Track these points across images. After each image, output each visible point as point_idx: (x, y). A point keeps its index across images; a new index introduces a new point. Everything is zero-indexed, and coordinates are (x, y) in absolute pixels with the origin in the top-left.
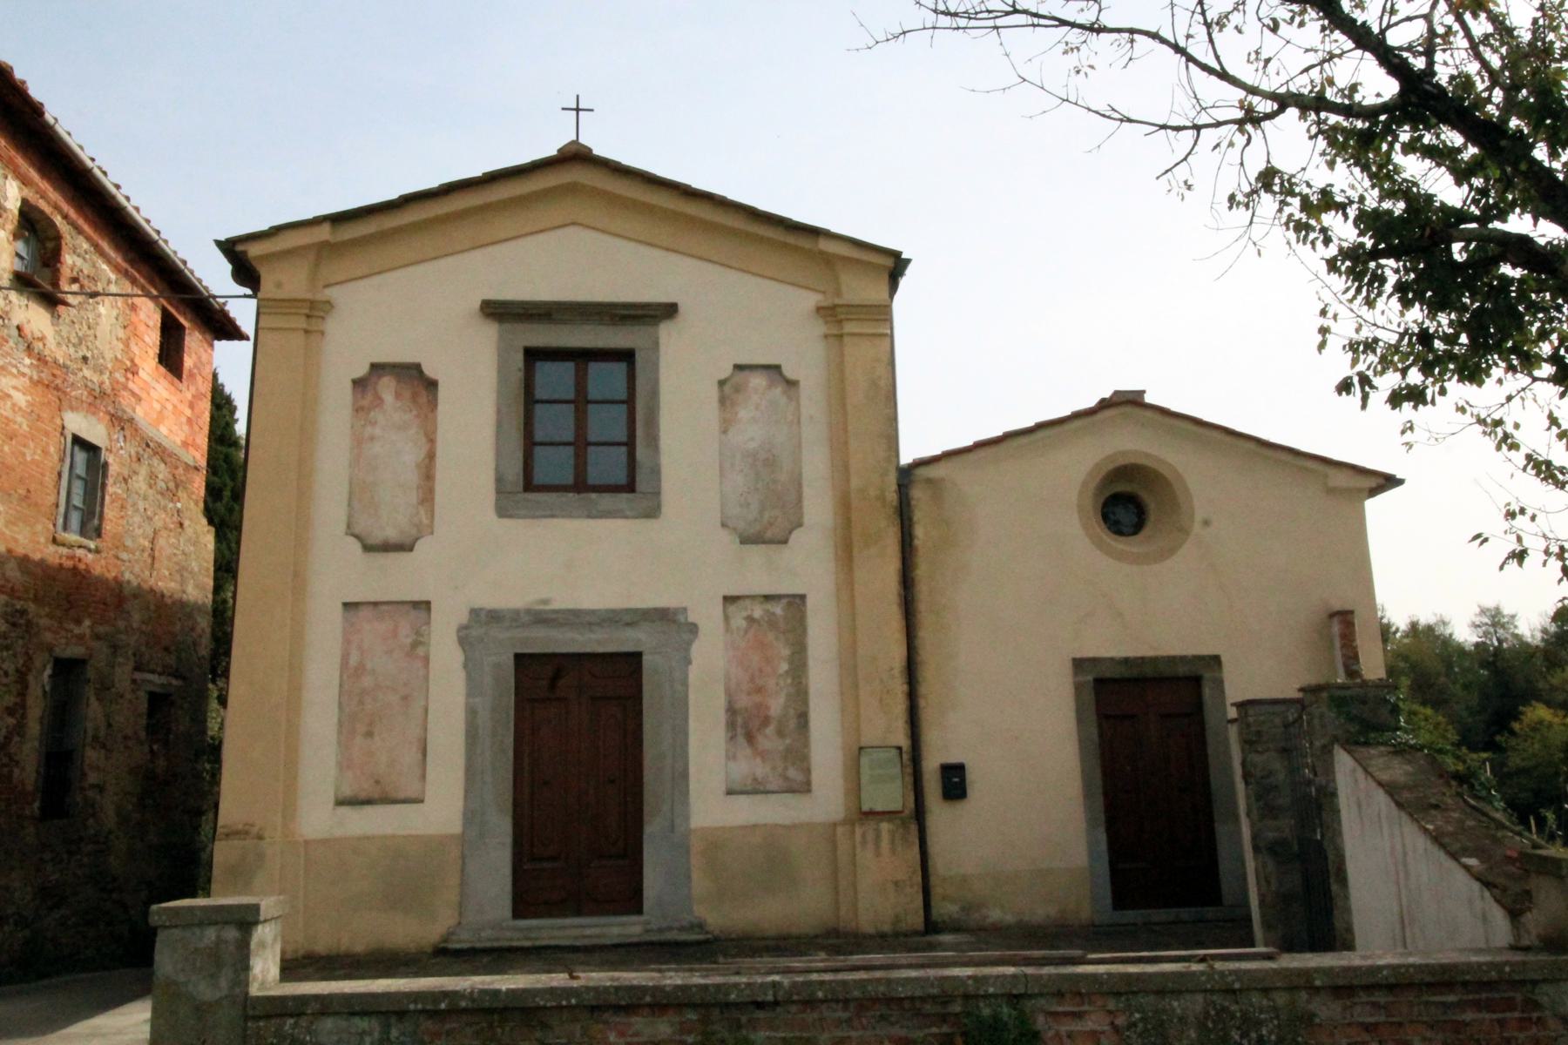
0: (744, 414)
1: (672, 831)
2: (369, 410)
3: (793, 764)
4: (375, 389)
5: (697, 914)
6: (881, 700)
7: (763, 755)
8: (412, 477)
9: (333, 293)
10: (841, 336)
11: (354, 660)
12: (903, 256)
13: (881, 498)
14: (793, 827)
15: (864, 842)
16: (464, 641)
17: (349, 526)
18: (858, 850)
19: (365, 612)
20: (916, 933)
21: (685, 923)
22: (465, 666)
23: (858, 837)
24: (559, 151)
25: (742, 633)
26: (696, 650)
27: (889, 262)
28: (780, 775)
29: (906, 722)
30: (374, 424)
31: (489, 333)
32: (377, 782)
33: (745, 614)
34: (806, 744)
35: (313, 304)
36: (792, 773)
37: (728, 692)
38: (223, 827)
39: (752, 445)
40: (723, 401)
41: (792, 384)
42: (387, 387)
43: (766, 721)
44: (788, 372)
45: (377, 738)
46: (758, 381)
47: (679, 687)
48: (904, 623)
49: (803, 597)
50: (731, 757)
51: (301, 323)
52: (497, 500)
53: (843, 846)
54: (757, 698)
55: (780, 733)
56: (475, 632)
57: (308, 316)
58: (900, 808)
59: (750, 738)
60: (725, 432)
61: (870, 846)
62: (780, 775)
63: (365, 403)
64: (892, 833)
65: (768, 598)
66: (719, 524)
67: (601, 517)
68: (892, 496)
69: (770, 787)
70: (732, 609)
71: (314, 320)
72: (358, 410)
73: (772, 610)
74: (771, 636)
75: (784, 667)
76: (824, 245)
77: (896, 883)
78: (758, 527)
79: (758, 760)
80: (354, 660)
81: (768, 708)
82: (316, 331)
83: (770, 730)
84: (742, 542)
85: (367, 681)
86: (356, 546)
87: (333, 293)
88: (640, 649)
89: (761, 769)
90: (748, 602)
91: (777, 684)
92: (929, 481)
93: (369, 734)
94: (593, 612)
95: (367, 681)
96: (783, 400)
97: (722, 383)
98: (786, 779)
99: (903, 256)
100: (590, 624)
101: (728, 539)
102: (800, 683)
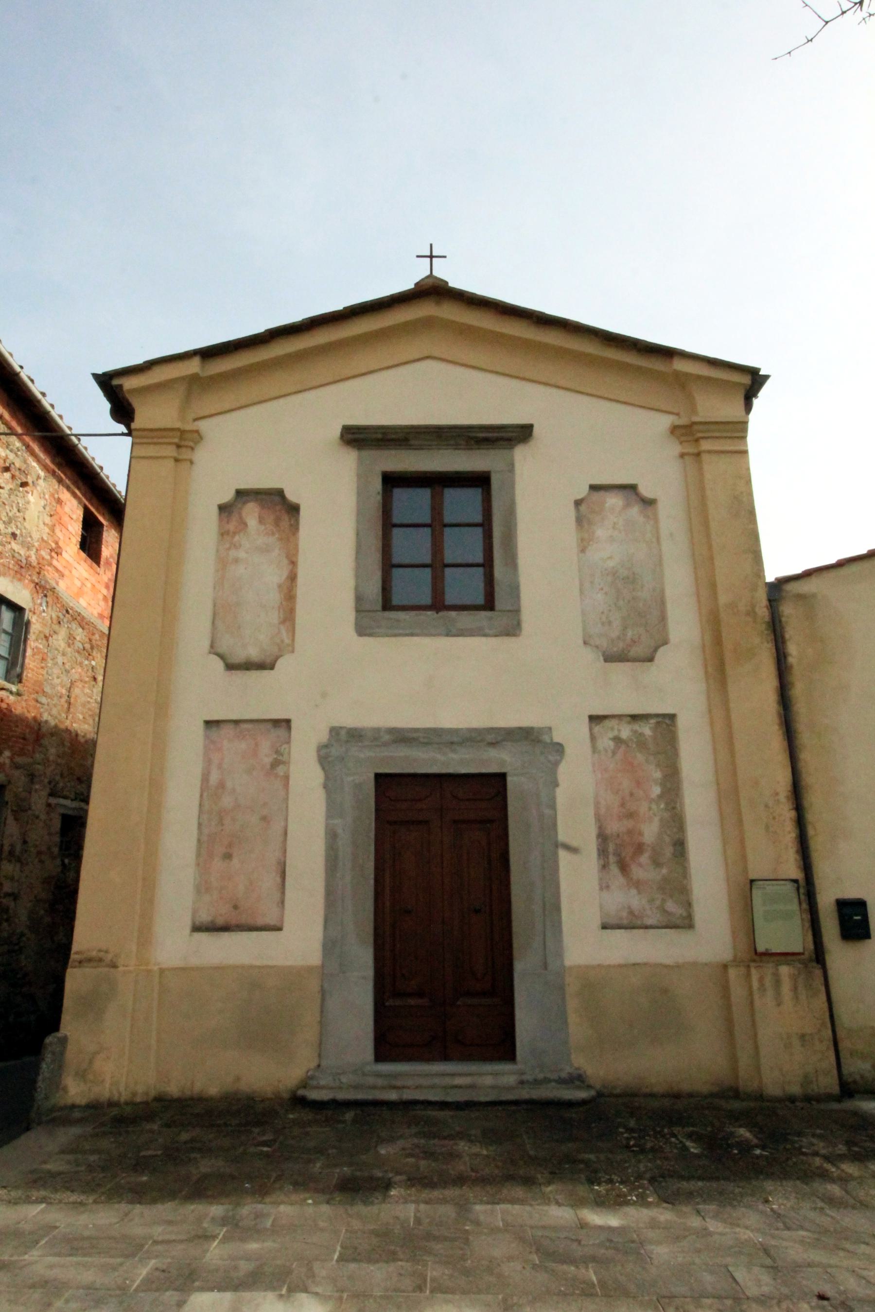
0: (601, 533)
1: (546, 968)
2: (235, 533)
3: (671, 896)
4: (240, 514)
5: (576, 1065)
6: (767, 827)
7: (638, 885)
8: (274, 597)
9: (204, 426)
10: (698, 454)
11: (214, 778)
12: (761, 373)
13: (751, 612)
14: (678, 966)
15: (762, 988)
16: (325, 758)
17: (212, 646)
18: (756, 997)
19: (227, 731)
20: (830, 1097)
21: (564, 1075)
22: (325, 786)
23: (755, 984)
24: (417, 284)
25: (610, 754)
26: (563, 771)
27: (746, 380)
28: (657, 908)
29: (797, 852)
30: (237, 546)
31: (350, 458)
32: (236, 907)
33: (611, 735)
34: (685, 873)
35: (182, 432)
36: (671, 906)
37: (598, 818)
38: (77, 953)
39: (611, 564)
40: (580, 521)
41: (649, 503)
42: (251, 512)
43: (640, 848)
44: (646, 491)
45: (235, 861)
46: (614, 501)
47: (547, 811)
48: (786, 743)
49: (672, 717)
50: (604, 887)
51: (171, 451)
52: (356, 618)
53: (737, 992)
54: (629, 824)
55: (657, 863)
56: (335, 751)
57: (179, 446)
58: (801, 951)
59: (624, 868)
60: (583, 550)
61: (770, 993)
62: (657, 908)
63: (231, 527)
64: (794, 979)
65: (635, 718)
66: (581, 642)
67: (458, 636)
68: (763, 611)
69: (649, 922)
70: (597, 729)
71: (184, 450)
72: (223, 534)
73: (640, 731)
74: (640, 757)
75: (656, 790)
76: (679, 365)
77: (802, 1037)
78: (621, 645)
79: (634, 891)
80: (214, 778)
81: (641, 834)
82: (186, 460)
83: (644, 859)
84: (606, 660)
85: (227, 801)
86: (220, 665)
87: (204, 426)
88: (503, 771)
89: (636, 901)
90: (613, 723)
91: (650, 809)
92: (801, 597)
93: (228, 856)
94: (455, 731)
95: (227, 801)
96: (641, 519)
97: (578, 503)
98: (665, 912)
99: (761, 373)
100: (452, 743)
101: (590, 658)
102: (674, 808)
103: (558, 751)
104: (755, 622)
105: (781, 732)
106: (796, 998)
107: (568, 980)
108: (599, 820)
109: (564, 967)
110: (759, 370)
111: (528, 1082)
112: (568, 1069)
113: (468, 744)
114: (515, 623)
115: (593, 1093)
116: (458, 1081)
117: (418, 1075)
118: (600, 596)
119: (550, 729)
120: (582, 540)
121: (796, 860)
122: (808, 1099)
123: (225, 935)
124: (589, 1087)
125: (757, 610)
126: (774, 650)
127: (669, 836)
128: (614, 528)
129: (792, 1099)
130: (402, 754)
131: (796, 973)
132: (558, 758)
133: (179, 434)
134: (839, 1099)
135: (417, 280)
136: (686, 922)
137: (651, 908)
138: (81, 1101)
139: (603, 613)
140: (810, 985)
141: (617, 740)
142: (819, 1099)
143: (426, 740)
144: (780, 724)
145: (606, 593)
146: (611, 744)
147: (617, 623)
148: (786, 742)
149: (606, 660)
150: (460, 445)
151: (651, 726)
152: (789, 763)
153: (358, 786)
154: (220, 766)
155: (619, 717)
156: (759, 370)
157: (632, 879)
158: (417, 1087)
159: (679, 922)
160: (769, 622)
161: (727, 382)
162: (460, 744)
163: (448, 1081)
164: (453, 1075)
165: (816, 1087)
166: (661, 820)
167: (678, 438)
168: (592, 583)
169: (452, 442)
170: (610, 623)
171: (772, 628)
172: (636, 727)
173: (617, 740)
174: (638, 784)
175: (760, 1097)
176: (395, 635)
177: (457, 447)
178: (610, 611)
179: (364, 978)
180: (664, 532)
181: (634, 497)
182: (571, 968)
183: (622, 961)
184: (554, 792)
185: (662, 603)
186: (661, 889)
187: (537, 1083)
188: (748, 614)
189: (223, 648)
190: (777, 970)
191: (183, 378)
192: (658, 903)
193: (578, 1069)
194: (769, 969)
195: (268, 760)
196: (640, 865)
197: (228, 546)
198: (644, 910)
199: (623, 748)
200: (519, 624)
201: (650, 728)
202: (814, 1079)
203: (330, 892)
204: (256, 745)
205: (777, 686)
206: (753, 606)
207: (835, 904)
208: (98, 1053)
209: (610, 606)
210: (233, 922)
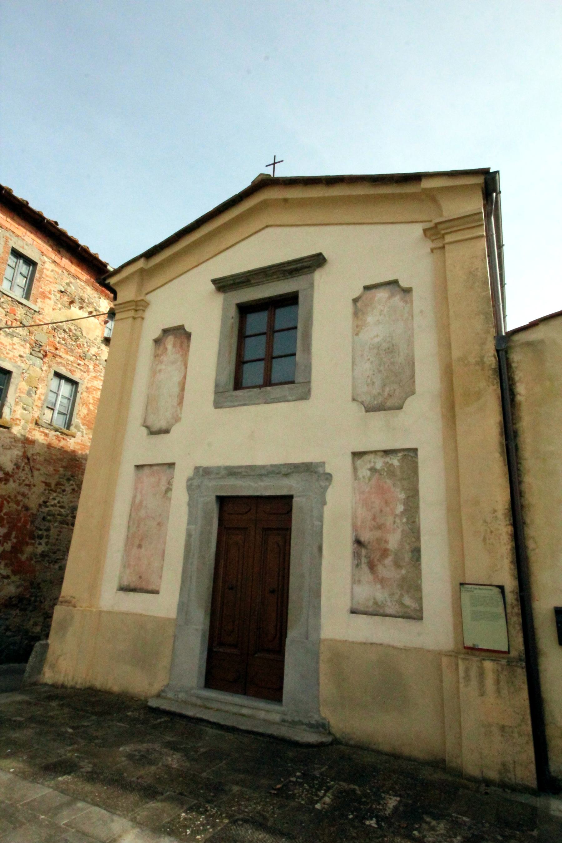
0: (370, 319)
1: (307, 639)
2: (161, 355)
3: (408, 592)
4: (164, 344)
5: (323, 715)
6: (484, 540)
7: (382, 581)
8: (176, 390)
9: (149, 298)
10: (443, 247)
11: (137, 501)
12: (491, 171)
13: (481, 363)
14: (405, 650)
15: (467, 677)
16: (190, 488)
17: (145, 422)
18: (461, 686)
19: (147, 471)
20: (525, 789)
21: (313, 722)
22: (189, 505)
23: (461, 673)
24: (252, 182)
25: (367, 481)
27: (480, 180)
28: (396, 601)
29: (512, 562)
30: (161, 362)
31: (220, 298)
32: (140, 577)
33: (369, 466)
34: (419, 575)
35: (136, 303)
36: (407, 601)
37: (355, 528)
38: (63, 597)
39: (376, 340)
40: (356, 314)
41: (407, 291)
42: (170, 342)
43: (385, 553)
44: (404, 284)
45: (143, 549)
46: (382, 294)
47: (317, 523)
48: (506, 469)
49: (415, 451)
50: (355, 581)
51: (132, 313)
52: (215, 398)
53: (448, 677)
54: (378, 534)
55: (397, 565)
56: (196, 482)
57: (136, 310)
58: (505, 649)
59: (372, 567)
60: (357, 334)
61: (474, 683)
62: (396, 601)
63: (160, 352)
64: (498, 673)
65: (387, 452)
66: (350, 398)
67: (272, 403)
68: (491, 360)
69: (389, 611)
70: (359, 462)
71: (139, 312)
72: (156, 356)
73: (390, 462)
74: (389, 482)
75: (400, 508)
76: (426, 184)
77: (503, 728)
78: (380, 399)
79: (379, 586)
80: (137, 501)
81: (386, 542)
82: (139, 317)
83: (388, 561)
84: (367, 411)
85: (142, 513)
86: (144, 431)
87: (149, 298)
88: (291, 493)
89: (381, 595)
90: (372, 457)
91: (394, 522)
92: (529, 344)
93: (140, 546)
94: (263, 467)
95: (142, 513)
96: (401, 304)
97: (355, 301)
98: (402, 604)
99: (491, 171)
100: (261, 475)
101: (356, 410)
102: (414, 522)
103: (327, 479)
104: (483, 369)
105: (502, 459)
106: (498, 691)
107: (322, 648)
108: (356, 530)
109: (320, 639)
110: (489, 169)
111: (287, 721)
112: (316, 717)
113: (271, 475)
114: (307, 390)
115: (329, 739)
116: (244, 711)
117: (221, 702)
118: (367, 366)
119: (324, 463)
120: (357, 326)
121: (510, 569)
122: (503, 785)
123: (132, 594)
124: (330, 733)
125: (485, 359)
126: (499, 391)
127: (409, 544)
128: (380, 315)
129: (488, 783)
130: (232, 483)
131: (500, 669)
132: (327, 484)
133: (134, 303)
134: (535, 793)
135: (252, 181)
136: (418, 614)
137: (391, 601)
138: (50, 682)
139: (368, 376)
140: (512, 683)
141: (373, 470)
142: (514, 788)
143: (245, 474)
144: (502, 453)
145: (372, 363)
146: (369, 473)
147: (378, 383)
148: (507, 467)
149: (367, 411)
150: (280, 277)
151: (399, 458)
152: (508, 485)
153: (206, 504)
154: (141, 492)
155: (375, 452)
156: (489, 169)
157: (377, 576)
158: (217, 710)
159: (412, 614)
160: (495, 369)
161: (466, 186)
162: (267, 475)
163: (235, 709)
164: (242, 706)
165: (513, 776)
166: (403, 531)
167: (430, 238)
168: (362, 355)
169: (275, 277)
170: (373, 383)
171: (498, 373)
172: (387, 459)
173: (373, 470)
174: (387, 503)
175: (459, 773)
176: (234, 406)
177: (278, 279)
178: (374, 374)
179: (197, 630)
180: (416, 310)
181: (397, 289)
182: (325, 640)
183: (363, 640)
184: (323, 509)
185: (412, 365)
186: (401, 586)
187: (293, 723)
188: (477, 363)
189: (149, 423)
190: (482, 664)
191: (135, 272)
192: (397, 596)
193: (325, 719)
194: (474, 661)
195: (164, 488)
196: (384, 566)
197: (157, 363)
198: (386, 601)
199: (377, 475)
200: (309, 391)
201: (398, 460)
202: (512, 769)
203: (184, 571)
204: (159, 479)
205: (500, 422)
206: (482, 357)
207: (553, 611)
208: (60, 656)
209: (374, 371)
210: (139, 587)
